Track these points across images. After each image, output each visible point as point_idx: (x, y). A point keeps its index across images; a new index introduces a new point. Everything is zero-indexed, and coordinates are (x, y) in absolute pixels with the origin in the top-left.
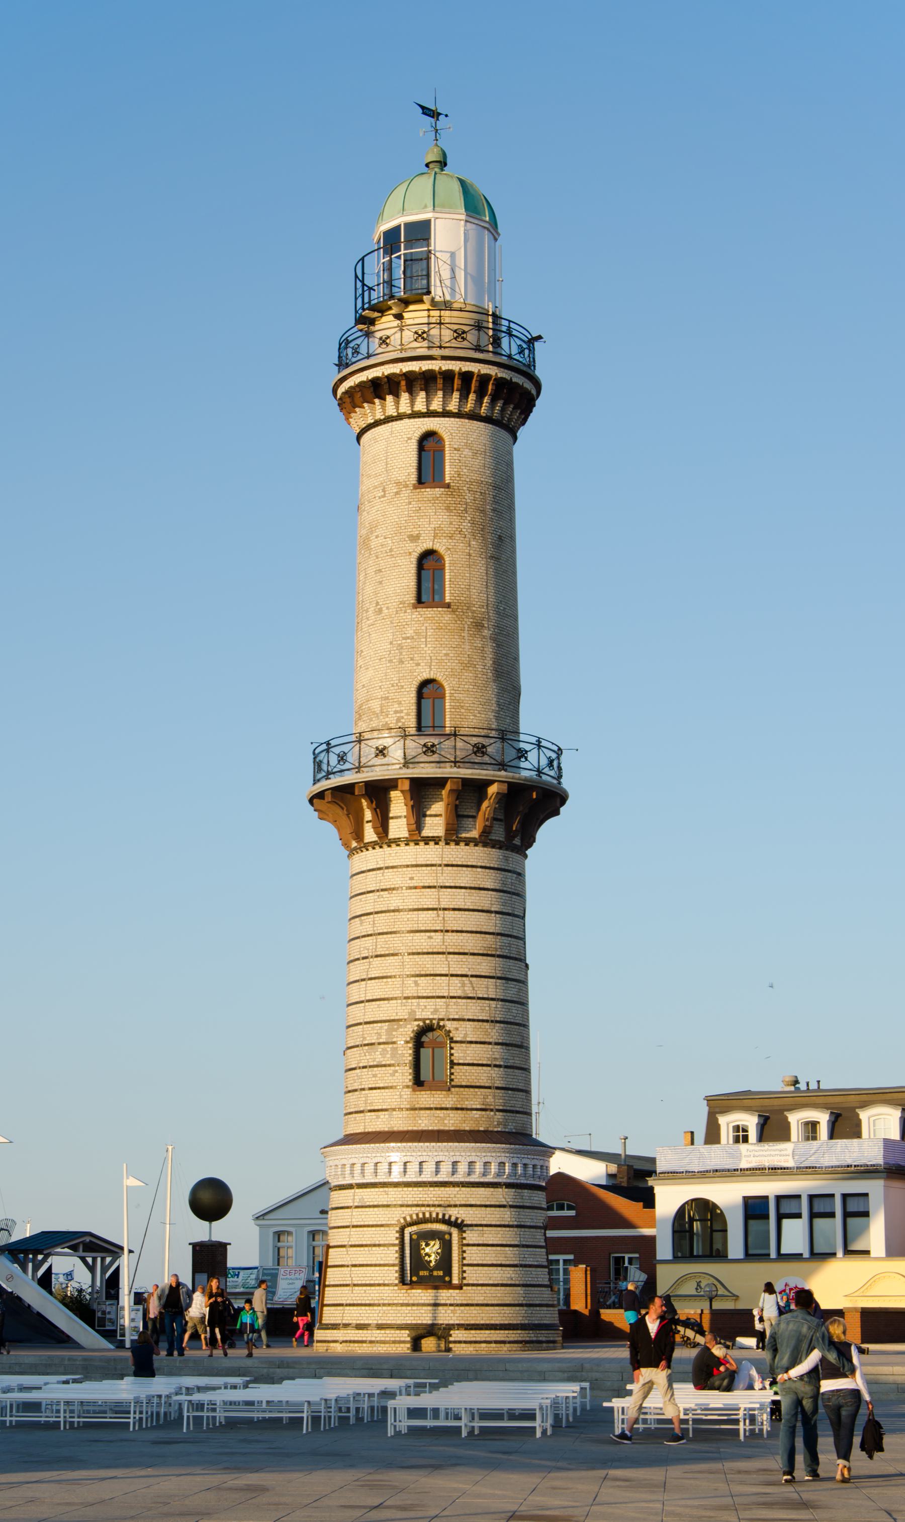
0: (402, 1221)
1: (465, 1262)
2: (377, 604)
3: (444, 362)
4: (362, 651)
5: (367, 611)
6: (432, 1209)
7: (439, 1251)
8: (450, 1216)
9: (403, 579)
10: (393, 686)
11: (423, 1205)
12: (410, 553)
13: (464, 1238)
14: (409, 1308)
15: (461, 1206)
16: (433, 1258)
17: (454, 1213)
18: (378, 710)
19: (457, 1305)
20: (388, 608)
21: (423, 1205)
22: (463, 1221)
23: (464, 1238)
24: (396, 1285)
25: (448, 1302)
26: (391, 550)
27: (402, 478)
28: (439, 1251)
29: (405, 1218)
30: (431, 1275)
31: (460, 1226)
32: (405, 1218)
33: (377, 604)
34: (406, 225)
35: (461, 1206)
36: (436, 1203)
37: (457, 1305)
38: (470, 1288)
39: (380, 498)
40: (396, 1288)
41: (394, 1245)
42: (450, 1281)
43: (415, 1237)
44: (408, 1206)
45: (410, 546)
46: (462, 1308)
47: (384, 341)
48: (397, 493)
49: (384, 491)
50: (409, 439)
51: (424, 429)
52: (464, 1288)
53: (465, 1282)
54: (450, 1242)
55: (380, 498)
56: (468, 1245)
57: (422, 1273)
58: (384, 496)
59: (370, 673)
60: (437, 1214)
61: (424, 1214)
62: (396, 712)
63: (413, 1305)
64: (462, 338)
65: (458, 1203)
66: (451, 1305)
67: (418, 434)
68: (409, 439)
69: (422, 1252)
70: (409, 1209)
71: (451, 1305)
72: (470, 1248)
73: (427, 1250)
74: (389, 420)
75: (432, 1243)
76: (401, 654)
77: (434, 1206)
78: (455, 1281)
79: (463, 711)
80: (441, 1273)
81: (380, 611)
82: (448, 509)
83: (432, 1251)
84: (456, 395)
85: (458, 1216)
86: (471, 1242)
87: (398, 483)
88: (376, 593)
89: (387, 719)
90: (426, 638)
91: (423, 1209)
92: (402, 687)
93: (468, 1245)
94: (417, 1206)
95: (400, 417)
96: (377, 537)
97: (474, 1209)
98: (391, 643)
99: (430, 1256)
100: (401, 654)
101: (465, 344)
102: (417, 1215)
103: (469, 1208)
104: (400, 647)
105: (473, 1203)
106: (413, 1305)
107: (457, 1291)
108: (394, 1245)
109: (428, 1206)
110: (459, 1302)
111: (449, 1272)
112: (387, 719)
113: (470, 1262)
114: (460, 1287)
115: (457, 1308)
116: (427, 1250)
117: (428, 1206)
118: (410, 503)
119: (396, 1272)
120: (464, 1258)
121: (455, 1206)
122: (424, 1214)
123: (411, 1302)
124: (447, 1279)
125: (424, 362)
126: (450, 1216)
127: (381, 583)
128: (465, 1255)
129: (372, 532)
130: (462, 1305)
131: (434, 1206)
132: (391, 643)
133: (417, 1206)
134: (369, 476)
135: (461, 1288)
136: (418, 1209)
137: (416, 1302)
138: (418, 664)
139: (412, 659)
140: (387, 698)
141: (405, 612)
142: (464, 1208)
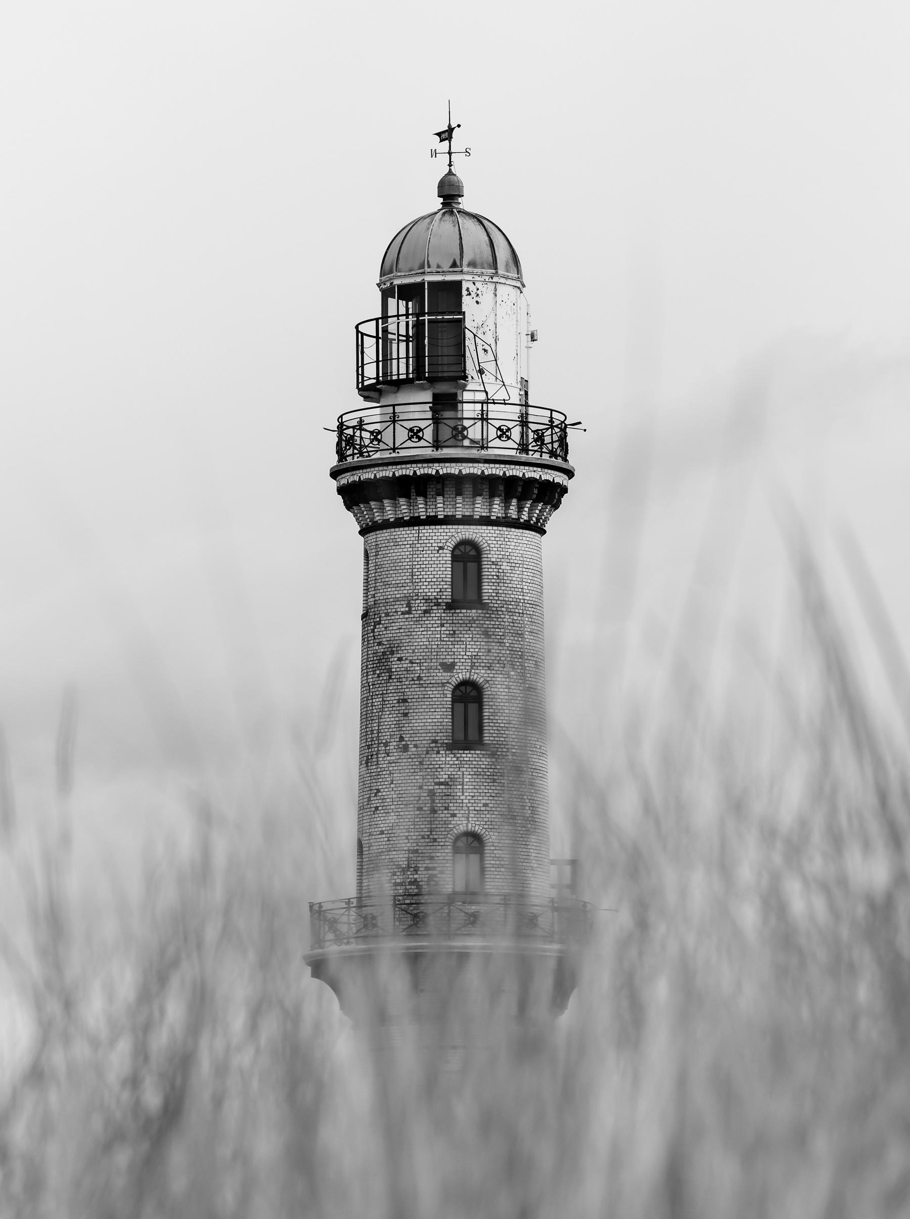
2: (402, 739)
3: (487, 465)
4: (378, 791)
5: (386, 744)
9: (434, 715)
10: (423, 838)
12: (443, 684)
18: (404, 864)
20: (416, 746)
26: (419, 678)
27: (432, 593)
33: (402, 739)
34: (429, 283)
39: (403, 613)
45: (443, 676)
47: (416, 434)
48: (426, 612)
49: (409, 605)
50: (441, 548)
51: (459, 537)
55: (403, 613)
58: (409, 612)
59: (392, 818)
62: (427, 869)
64: (507, 436)
67: (451, 544)
68: (441, 548)
74: (415, 522)
76: (433, 801)
79: (503, 870)
81: (406, 748)
82: (486, 634)
84: (497, 501)
87: (427, 600)
88: (399, 726)
89: (416, 876)
90: (463, 785)
92: (435, 840)
95: (433, 521)
96: (400, 659)
98: (421, 788)
100: (433, 801)
101: (510, 444)
104: (432, 793)
112: (416, 876)
118: (442, 625)
125: (464, 465)
127: (406, 715)
129: (392, 653)
132: (421, 788)
134: (386, 584)
138: (454, 815)
139: (447, 808)
140: (416, 851)
141: (438, 753)
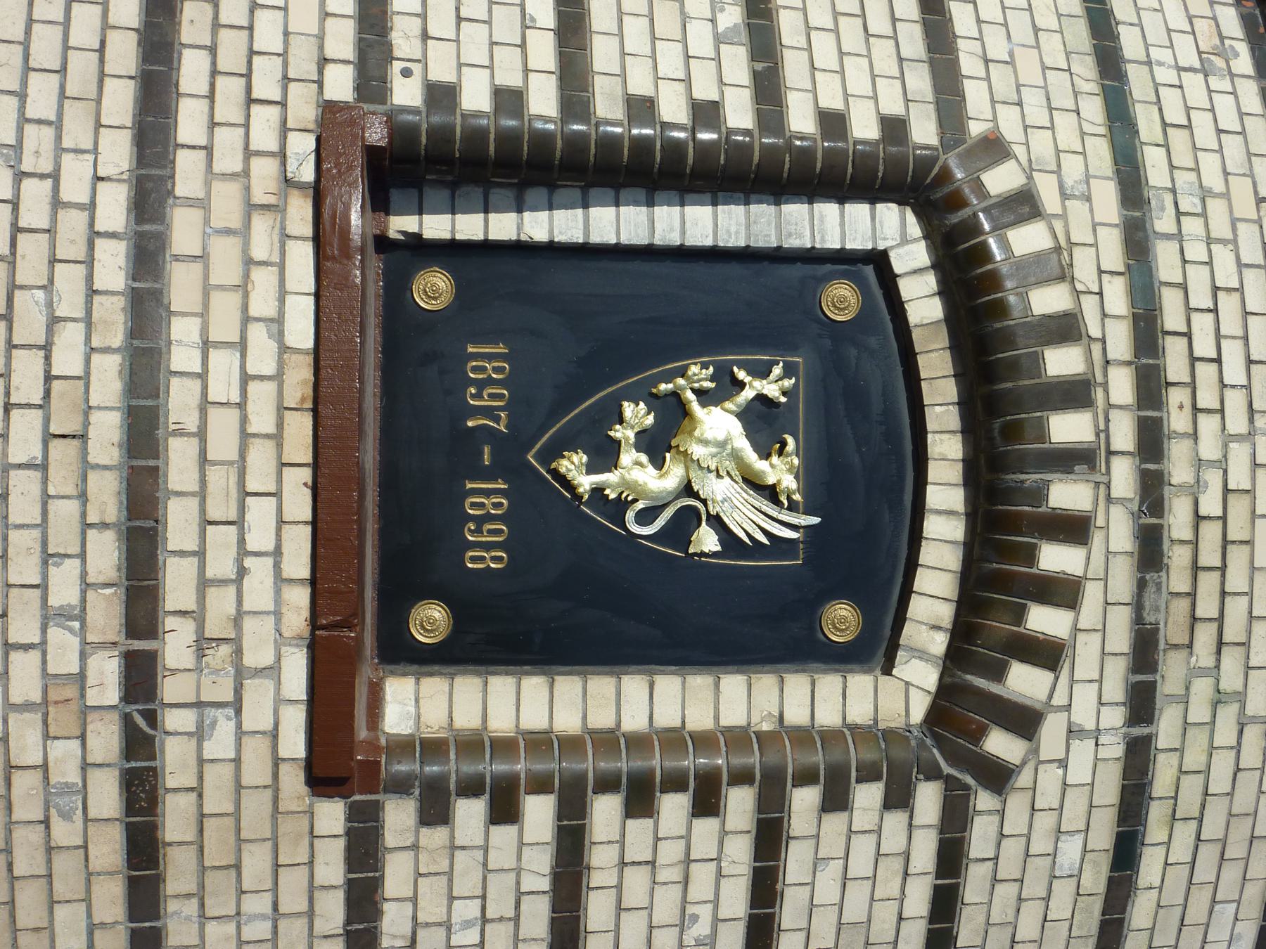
0: (1000, 180)
1: (605, 811)
6: (1123, 478)
7: (707, 540)
8: (1047, 654)
11: (1151, 387)
13: (836, 800)
14: (114, 208)
15: (1138, 757)
16: (637, 474)
17: (1079, 699)
19: (139, 744)
21: (1151, 387)
22: (998, 777)
23: (836, 800)
24: (371, 82)
25: (176, 646)
28: (707, 540)
29: (1023, 205)
30: (461, 453)
31: (963, 739)
32: (1023, 205)
35: (1138, 757)
36: (1178, 521)
37: (139, 744)
38: (332, 867)
40: (341, 85)
41: (768, 89)
42: (402, 653)
43: (842, 299)
44: (1137, 242)
46: (106, 796)
52: (332, 815)
53: (399, 816)
54: (800, 648)
56: (770, 837)
57: (487, 371)
60: (1074, 529)
61: (1075, 394)
63: (148, 256)
65: (1166, 728)
66: (141, 677)
69: (700, 373)
70: (1112, 252)
71: (141, 677)
72: (740, 852)
73: (718, 425)
75: (781, 472)
77: (1152, 490)
78: (409, 705)
80: (485, 555)
83: (716, 466)
85: (1052, 732)
86: (796, 862)
91: (1122, 386)
93: (770, 837)
94: (1147, 332)
97: (1096, 879)
99: (656, 446)
102: (1065, 328)
103: (1103, 836)
105: (1150, 867)
106: (148, 256)
107: (294, 744)
108: (768, 89)
109: (1151, 441)
110: (175, 760)
111: (496, 637)
113: (601, 858)
114: (339, 760)
115: (106, 740)
116: (718, 425)
117: (1151, 441)
119: (509, 99)
120: (640, 800)
121: (1141, 704)
122: (1075, 394)
123: (184, 231)
124: (431, 620)
126: (1047, 654)
128: (674, 806)
130: (141, 791)
131: (1152, 490)
133: (1147, 332)
135: (322, 780)
136: (1120, 342)
137: (182, 286)
142: (1109, 791)
